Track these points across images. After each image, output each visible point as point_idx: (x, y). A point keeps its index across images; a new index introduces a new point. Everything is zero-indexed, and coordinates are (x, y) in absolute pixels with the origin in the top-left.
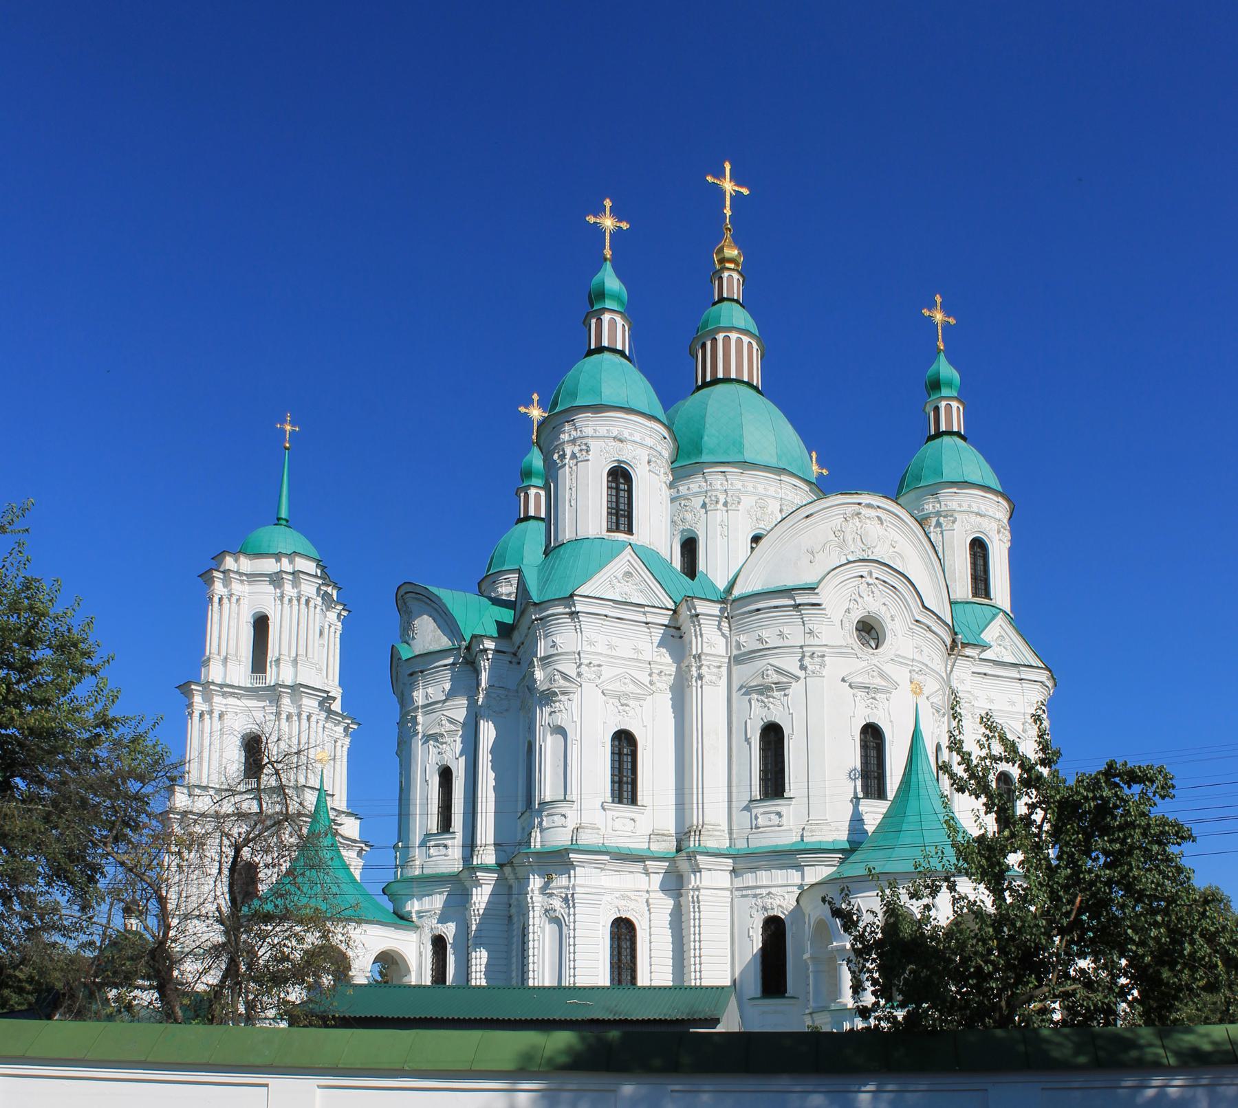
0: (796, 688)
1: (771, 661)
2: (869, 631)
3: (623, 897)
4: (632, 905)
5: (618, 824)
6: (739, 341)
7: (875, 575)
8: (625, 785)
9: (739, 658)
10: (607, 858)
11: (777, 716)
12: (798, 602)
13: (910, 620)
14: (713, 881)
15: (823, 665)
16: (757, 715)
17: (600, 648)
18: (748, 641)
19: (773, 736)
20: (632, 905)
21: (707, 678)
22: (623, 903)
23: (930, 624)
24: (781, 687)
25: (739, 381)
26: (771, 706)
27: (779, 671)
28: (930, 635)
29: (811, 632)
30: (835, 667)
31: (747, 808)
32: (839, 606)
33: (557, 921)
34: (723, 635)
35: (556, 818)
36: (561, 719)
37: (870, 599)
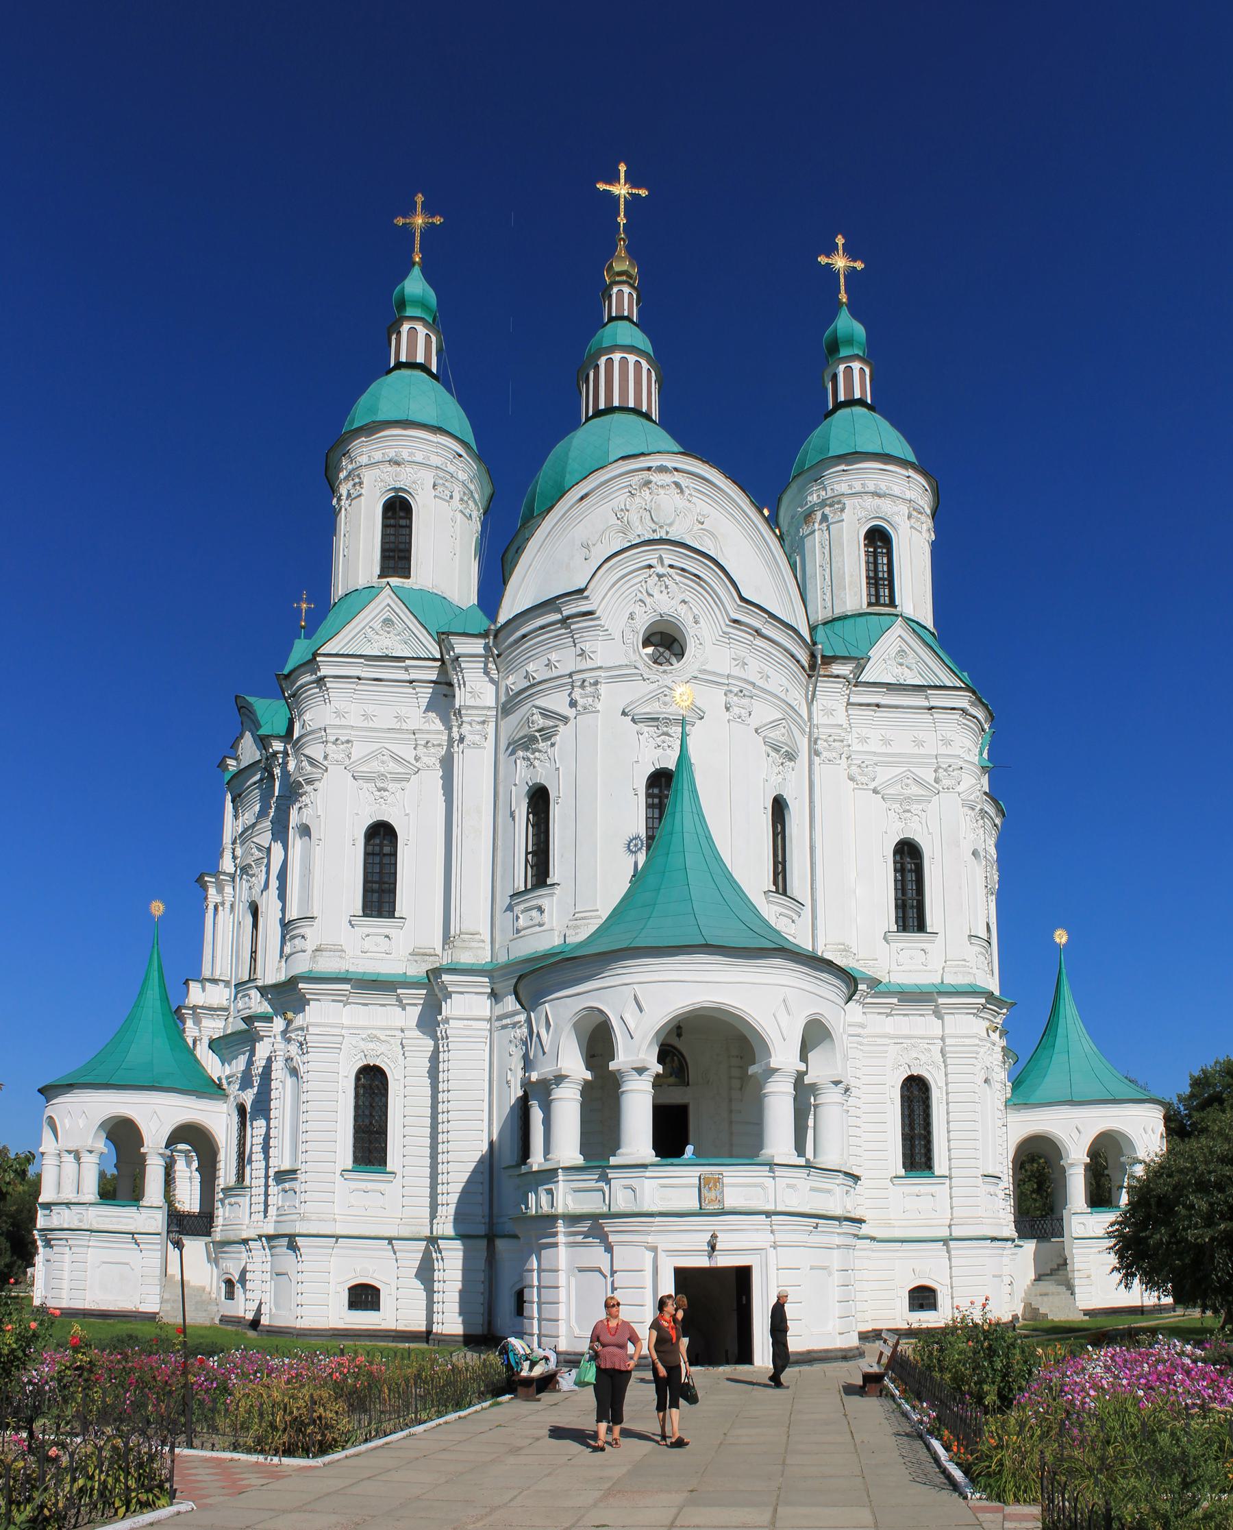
0: (564, 733)
1: (537, 703)
2: (666, 641)
3: (373, 1038)
4: (382, 1048)
5: (368, 944)
6: (624, 361)
7: (667, 562)
8: (379, 895)
9: (507, 708)
10: (348, 987)
11: (542, 776)
12: (565, 613)
13: (723, 621)
14: (468, 1006)
15: (597, 696)
16: (522, 776)
17: (353, 720)
18: (515, 681)
19: (539, 799)
20: (382, 1048)
21: (469, 738)
22: (371, 1045)
23: (757, 624)
24: (547, 734)
25: (624, 409)
26: (536, 763)
27: (546, 713)
28: (759, 642)
29: (582, 654)
30: (612, 697)
31: (510, 908)
32: (621, 614)
33: (294, 1072)
34: (492, 681)
35: (297, 941)
36: (307, 817)
37: (664, 596)
